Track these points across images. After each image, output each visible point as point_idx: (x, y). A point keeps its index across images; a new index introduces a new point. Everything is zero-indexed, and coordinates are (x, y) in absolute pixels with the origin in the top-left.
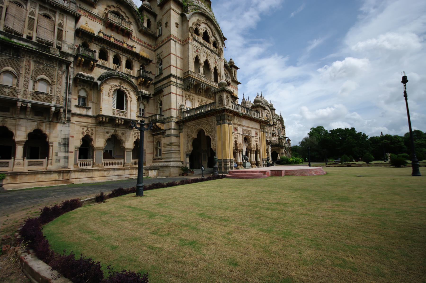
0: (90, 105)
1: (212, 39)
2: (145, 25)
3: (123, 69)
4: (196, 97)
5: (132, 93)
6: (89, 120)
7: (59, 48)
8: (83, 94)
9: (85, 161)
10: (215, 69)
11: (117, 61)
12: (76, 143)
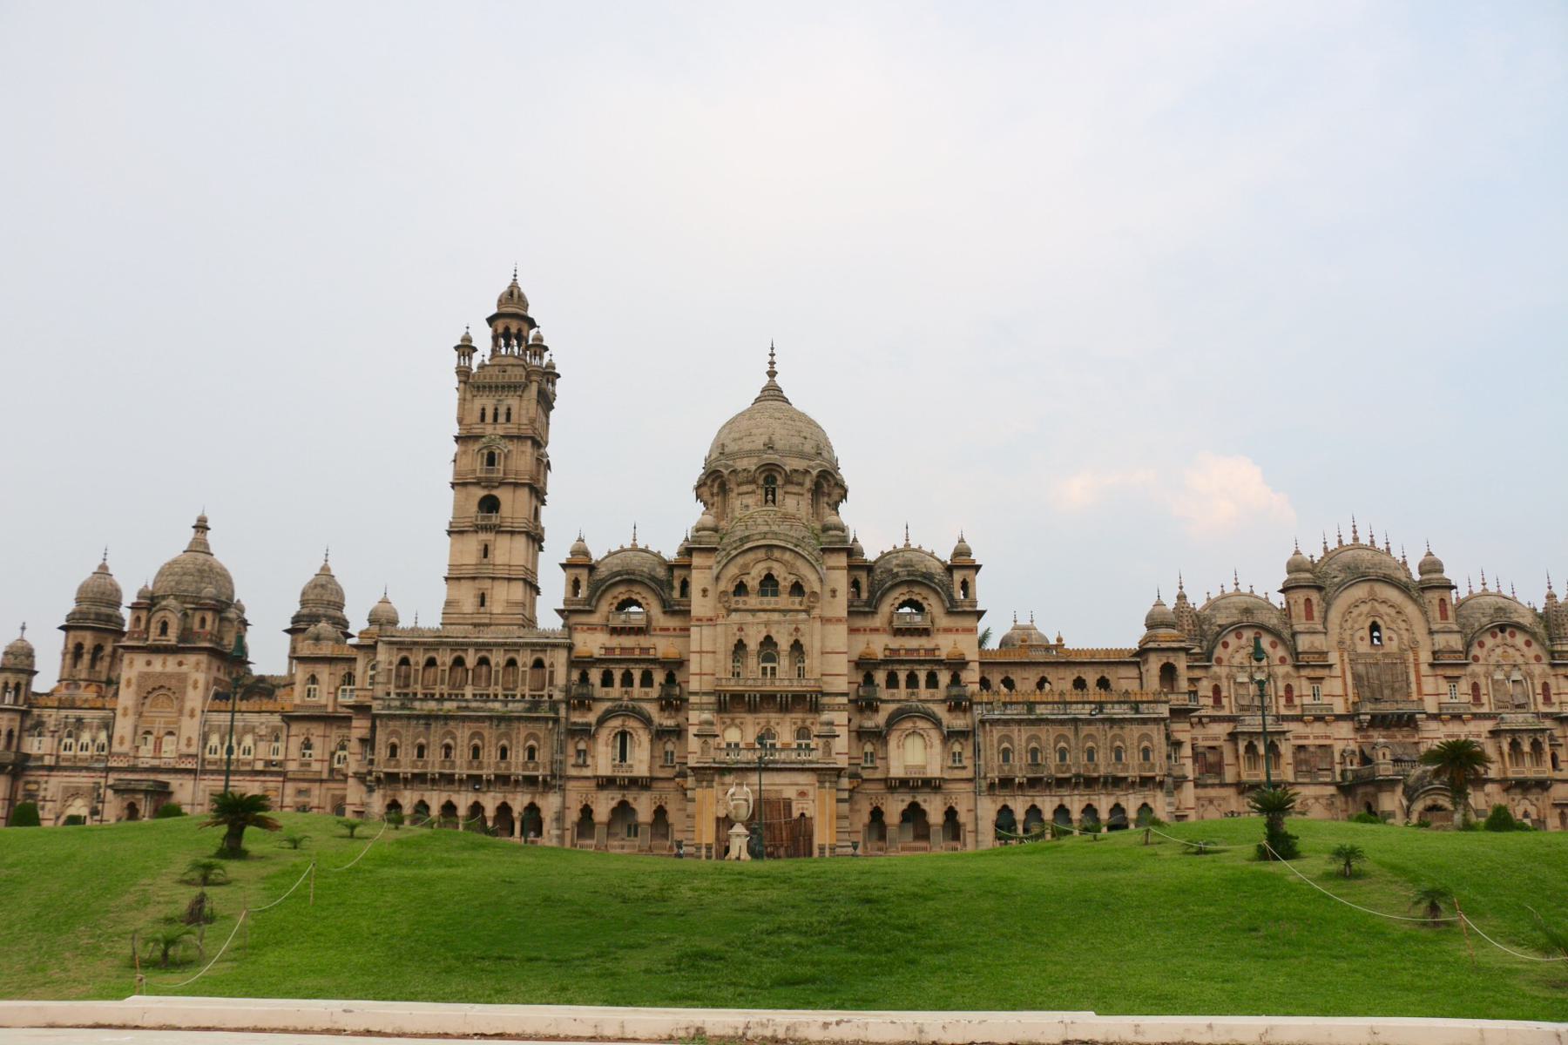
0: (589, 761)
1: (785, 579)
2: (676, 594)
3: (637, 690)
4: (749, 718)
5: (641, 732)
6: (587, 783)
7: (550, 696)
8: (582, 746)
9: (588, 842)
10: (797, 647)
11: (627, 680)
12: (573, 816)
